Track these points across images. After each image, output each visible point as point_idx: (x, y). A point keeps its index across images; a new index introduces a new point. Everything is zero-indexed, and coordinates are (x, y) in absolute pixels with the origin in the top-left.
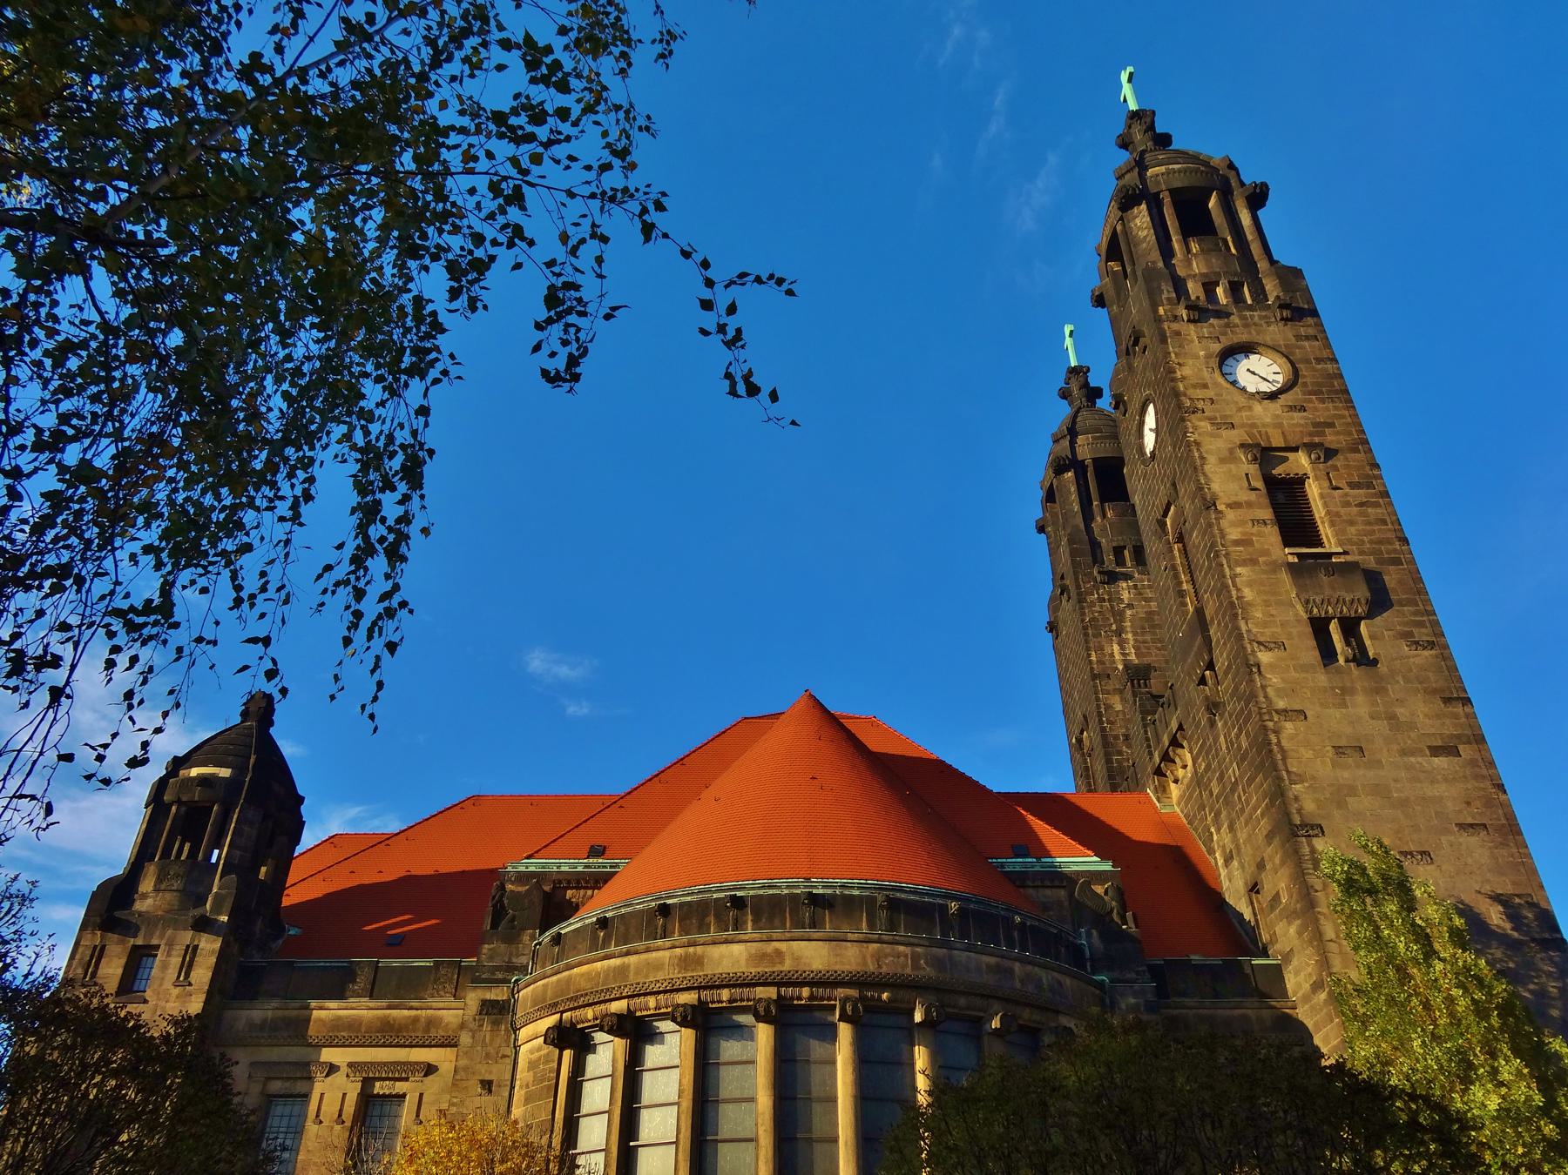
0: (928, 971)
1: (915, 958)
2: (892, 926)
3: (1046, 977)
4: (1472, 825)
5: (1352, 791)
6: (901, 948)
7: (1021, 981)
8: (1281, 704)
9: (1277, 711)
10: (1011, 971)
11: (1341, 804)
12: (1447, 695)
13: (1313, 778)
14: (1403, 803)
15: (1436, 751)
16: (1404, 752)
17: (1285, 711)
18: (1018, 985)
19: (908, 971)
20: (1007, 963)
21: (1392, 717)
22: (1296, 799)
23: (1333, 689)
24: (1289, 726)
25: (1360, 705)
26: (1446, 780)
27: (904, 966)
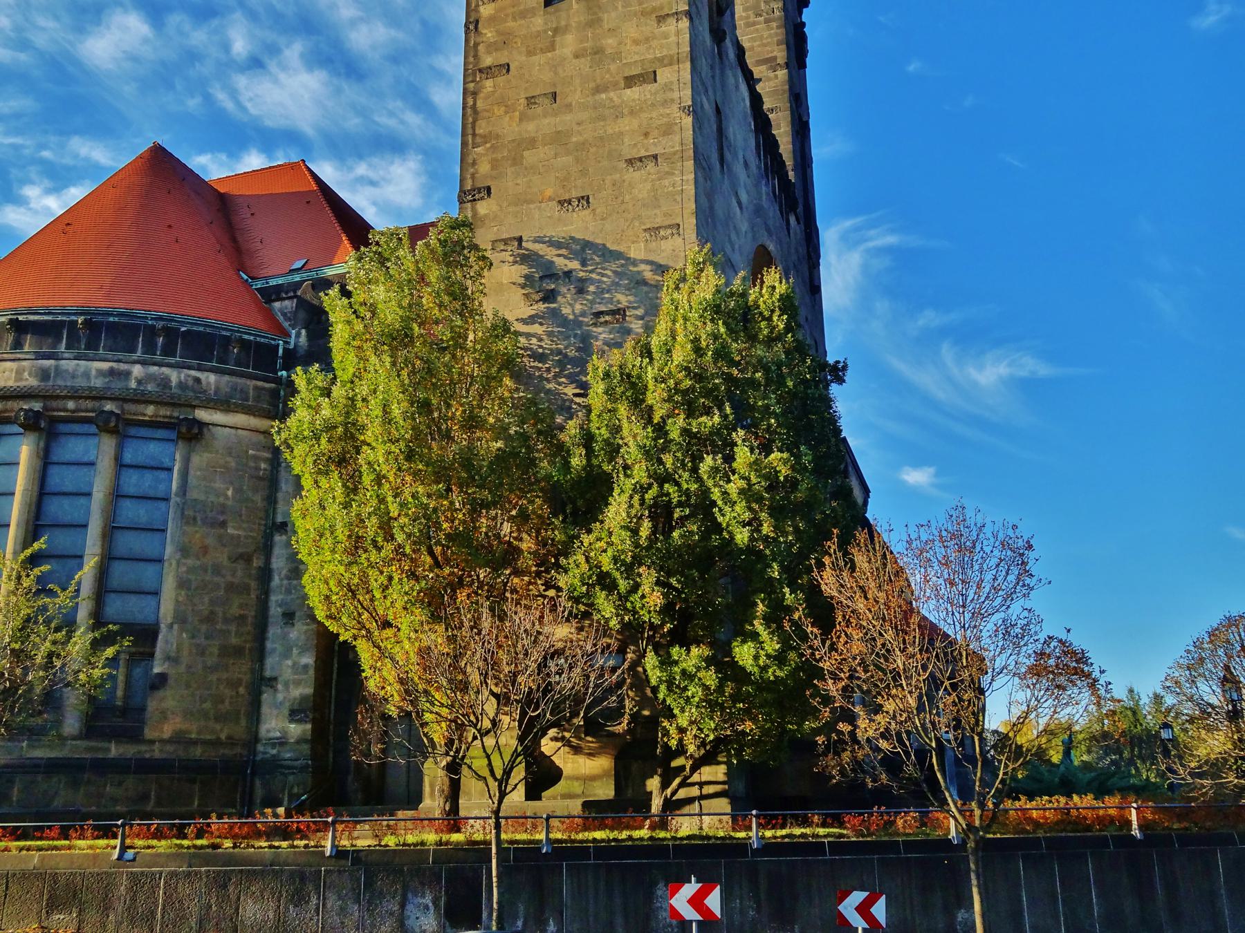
0: (31, 382)
1: (19, 373)
2: (18, 345)
3: (174, 376)
4: (640, 159)
5: (532, 143)
6: (8, 364)
7: (139, 382)
8: (487, 61)
9: (481, 71)
10: (128, 374)
11: (516, 161)
12: (666, 11)
13: (498, 136)
14: (583, 146)
15: (630, 81)
16: (598, 90)
17: (490, 68)
18: (133, 385)
19: (11, 383)
20: (123, 367)
21: (598, 51)
22: (474, 163)
23: (545, 31)
24: (489, 84)
25: (569, 44)
26: (632, 113)
27: (9, 379)
